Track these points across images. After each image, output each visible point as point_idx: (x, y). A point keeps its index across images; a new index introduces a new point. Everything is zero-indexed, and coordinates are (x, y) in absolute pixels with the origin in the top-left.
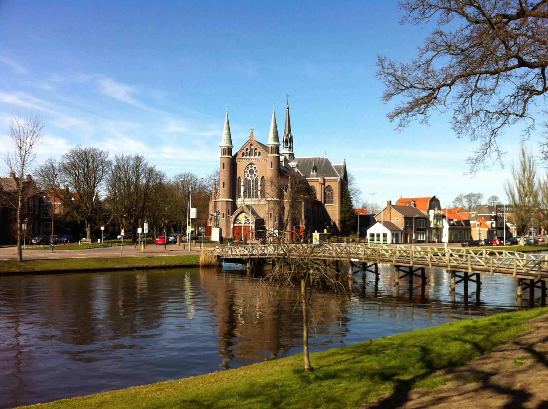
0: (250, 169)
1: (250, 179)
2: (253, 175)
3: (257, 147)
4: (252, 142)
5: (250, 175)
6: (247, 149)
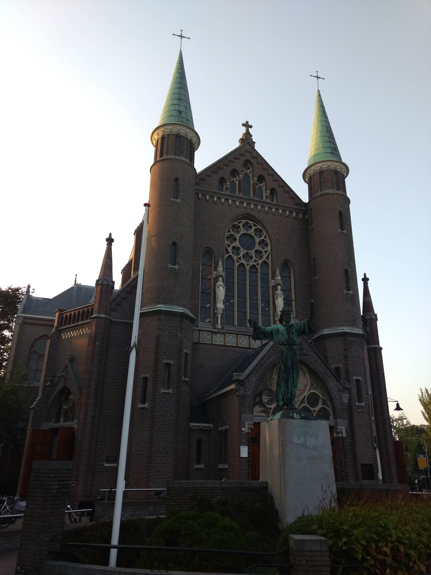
0: (243, 231)
2: (252, 252)
4: (248, 156)
5: (243, 252)
6: (234, 173)
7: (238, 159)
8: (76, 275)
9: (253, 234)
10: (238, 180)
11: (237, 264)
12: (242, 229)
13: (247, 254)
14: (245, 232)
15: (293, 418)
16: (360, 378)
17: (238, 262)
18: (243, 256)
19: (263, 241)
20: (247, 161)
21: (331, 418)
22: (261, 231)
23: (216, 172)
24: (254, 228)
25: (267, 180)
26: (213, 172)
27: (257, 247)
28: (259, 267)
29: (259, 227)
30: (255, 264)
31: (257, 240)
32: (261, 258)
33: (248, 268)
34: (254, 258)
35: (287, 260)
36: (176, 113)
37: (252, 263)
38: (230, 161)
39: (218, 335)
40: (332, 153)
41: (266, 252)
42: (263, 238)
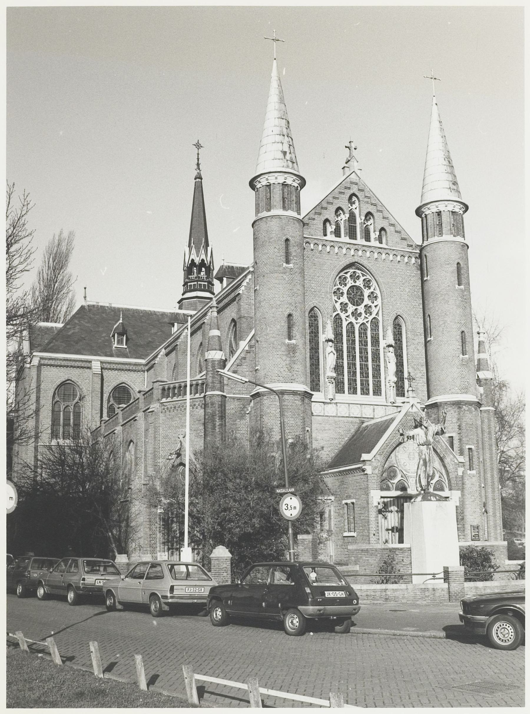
0: (350, 283)
1: (352, 319)
3: (372, 209)
7: (343, 193)
8: (85, 288)
9: (362, 286)
10: (343, 220)
11: (345, 324)
12: (350, 282)
13: (356, 309)
14: (354, 284)
15: (430, 500)
16: (472, 447)
17: (346, 320)
18: (352, 313)
19: (372, 293)
20: (354, 194)
21: (447, 489)
22: (369, 281)
23: (320, 214)
24: (362, 278)
25: (376, 218)
26: (316, 213)
27: (367, 301)
28: (369, 325)
29: (368, 277)
30: (365, 321)
31: (366, 292)
32: (371, 314)
33: (357, 327)
34: (364, 315)
35: (399, 315)
36: (281, 156)
37: (361, 320)
38: (334, 198)
39: (330, 405)
40: (450, 188)
41: (376, 306)
42: (372, 290)
